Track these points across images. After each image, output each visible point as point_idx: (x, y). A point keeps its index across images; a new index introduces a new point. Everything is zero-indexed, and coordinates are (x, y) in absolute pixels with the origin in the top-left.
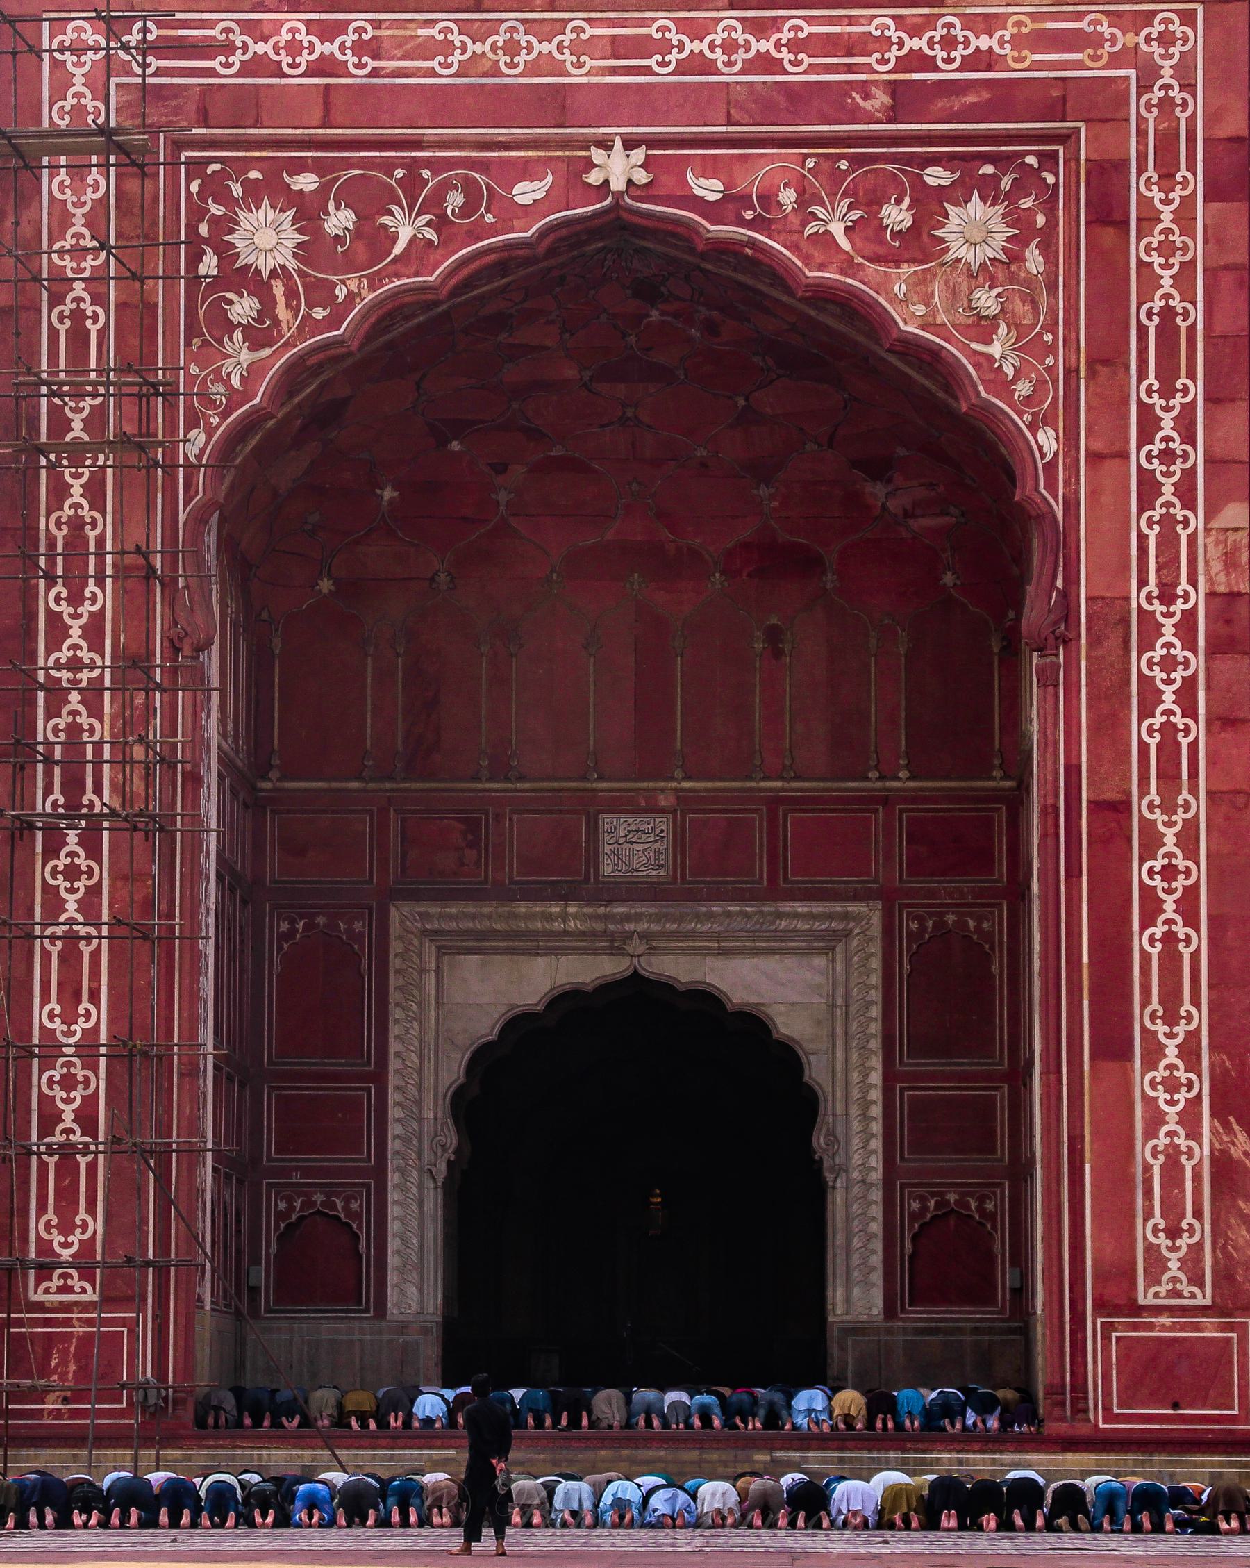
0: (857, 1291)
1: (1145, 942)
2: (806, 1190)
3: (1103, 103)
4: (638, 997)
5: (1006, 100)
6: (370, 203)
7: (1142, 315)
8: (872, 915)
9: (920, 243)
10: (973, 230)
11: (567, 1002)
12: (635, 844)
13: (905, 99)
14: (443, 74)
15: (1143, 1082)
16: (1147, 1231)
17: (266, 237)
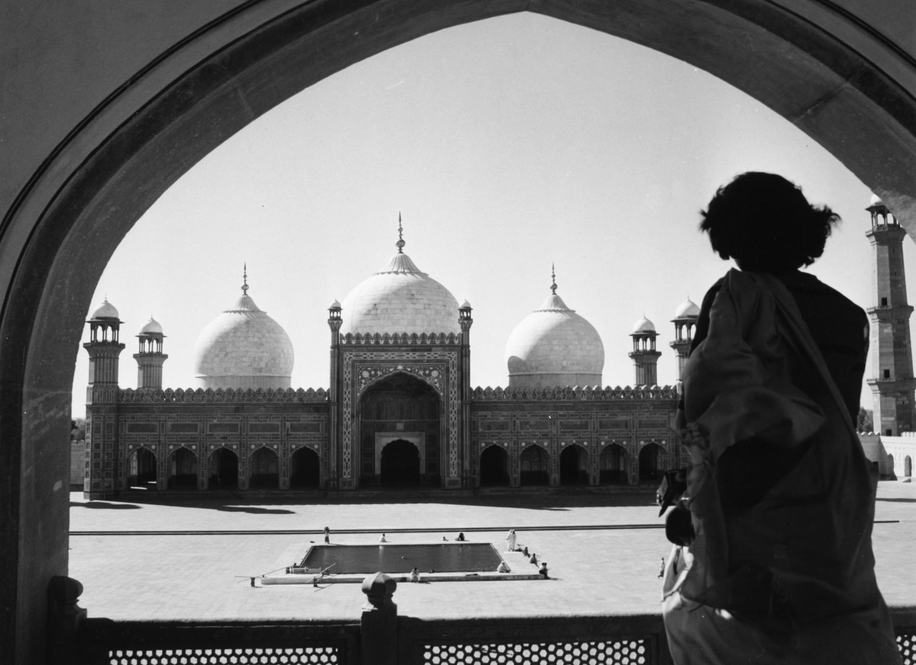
0: (423, 470)
1: (451, 442)
2: (418, 460)
3: (447, 362)
4: (400, 441)
5: (438, 361)
6: (376, 371)
7: (451, 382)
8: (424, 433)
9: (430, 375)
10: (435, 373)
11: (393, 442)
12: (400, 426)
13: (428, 361)
14: (383, 358)
15: (451, 456)
16: (451, 470)
17: (366, 374)
